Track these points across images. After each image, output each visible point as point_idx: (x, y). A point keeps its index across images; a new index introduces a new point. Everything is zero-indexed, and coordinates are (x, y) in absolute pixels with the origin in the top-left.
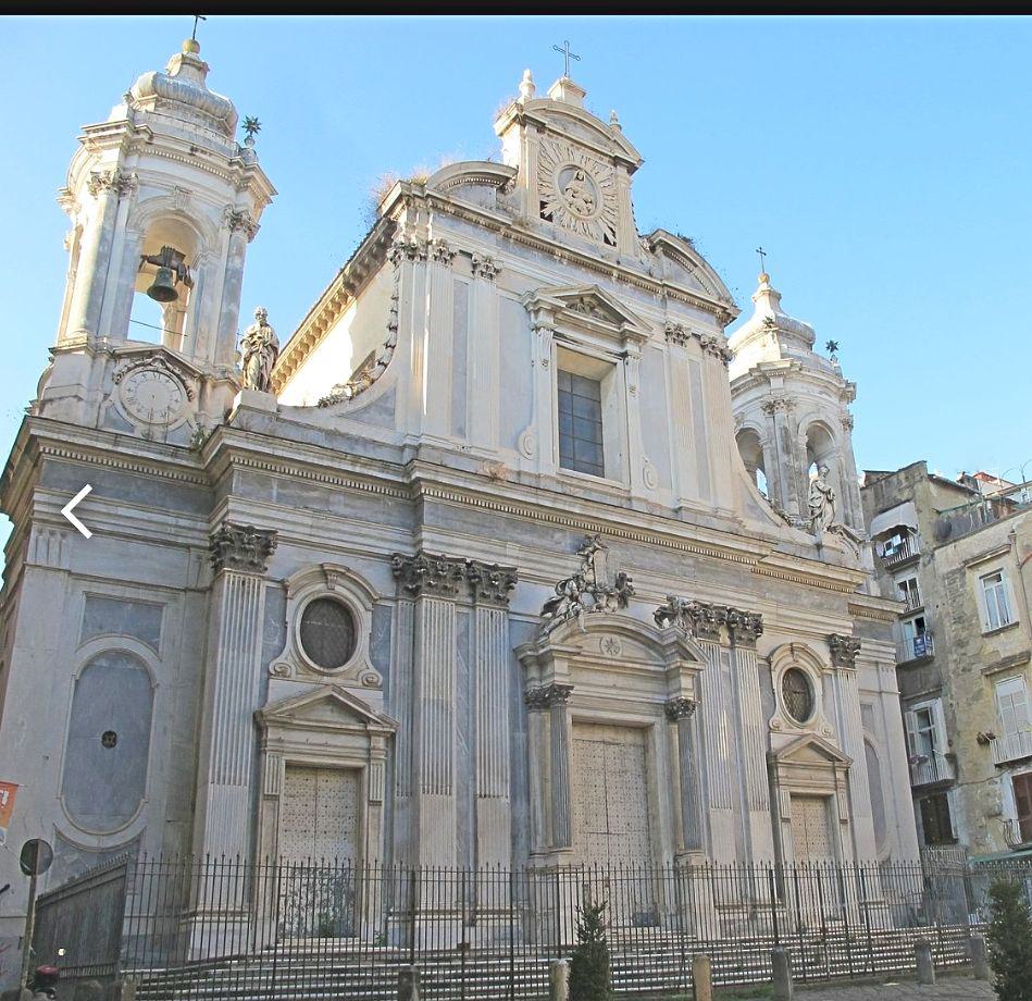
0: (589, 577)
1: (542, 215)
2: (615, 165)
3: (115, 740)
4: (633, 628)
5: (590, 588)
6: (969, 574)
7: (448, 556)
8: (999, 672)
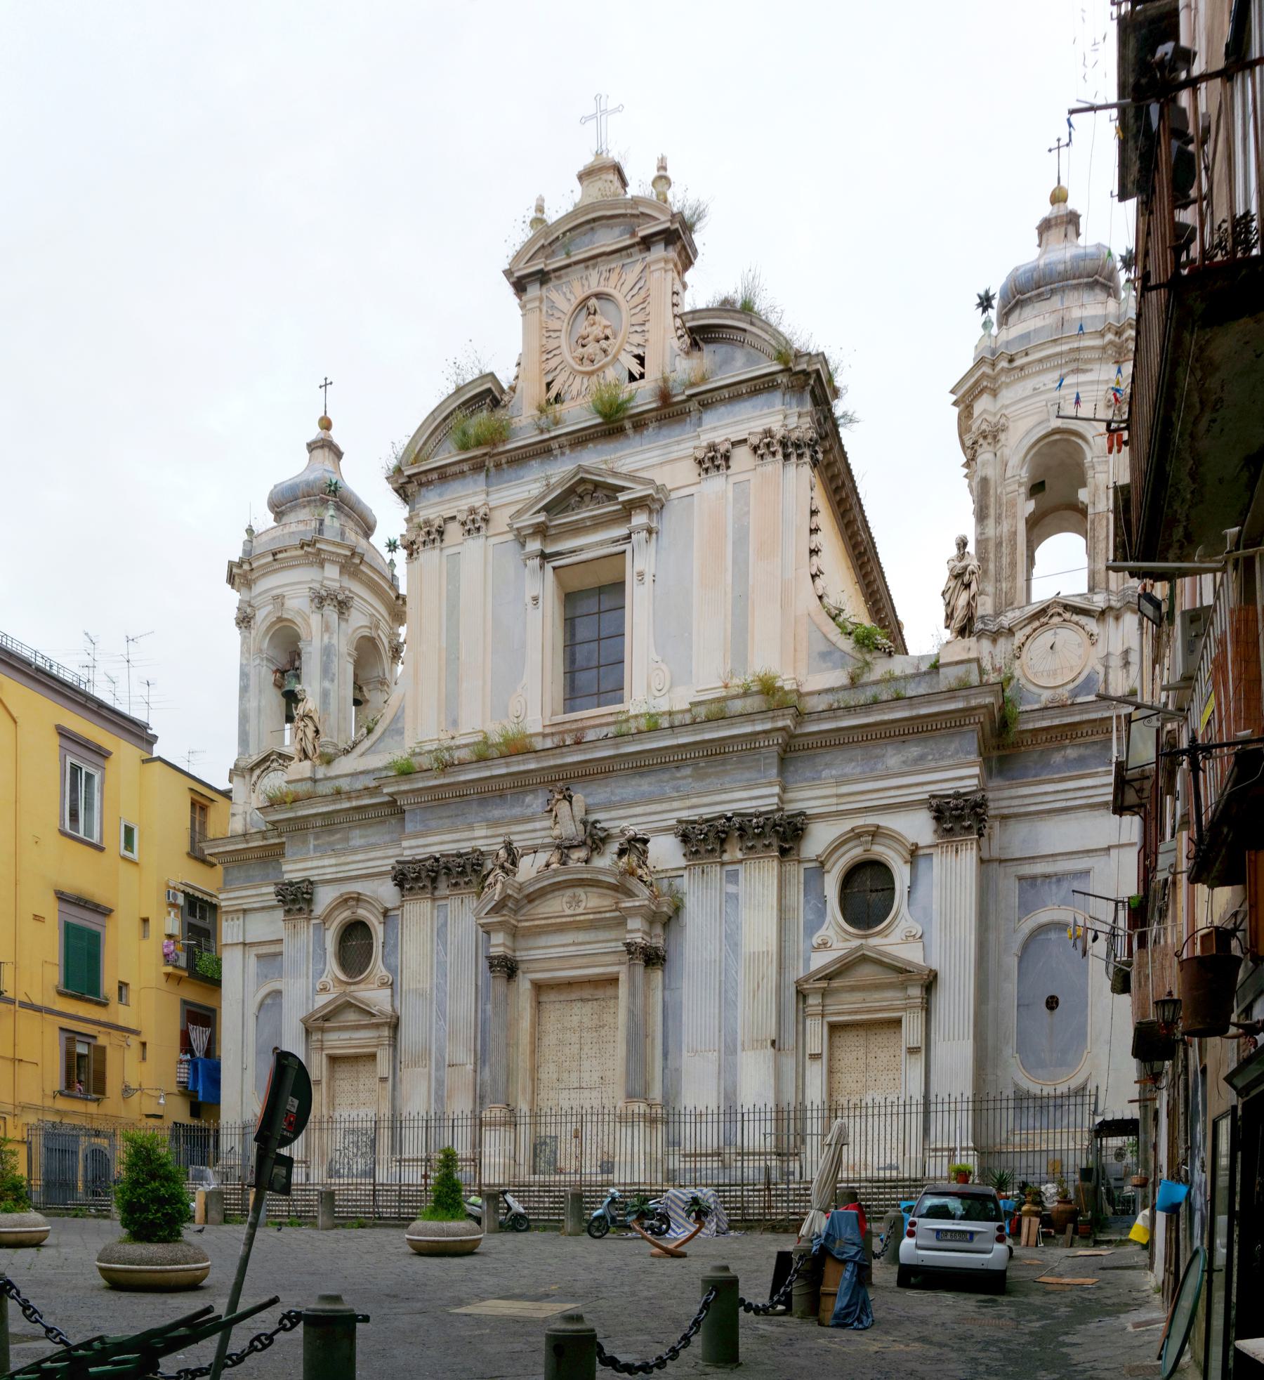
4: (589, 876)
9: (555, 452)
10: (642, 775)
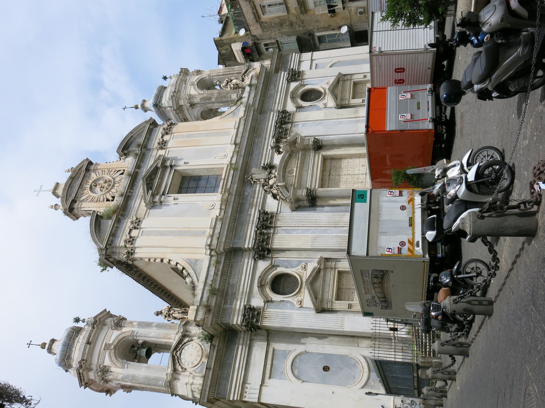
0: (262, 181)
1: (113, 200)
2: (89, 170)
3: (326, 367)
4: (284, 163)
5: (267, 180)
6: (262, 20)
7: (254, 237)
8: (304, 7)
9: (130, 195)
10: (252, 154)
